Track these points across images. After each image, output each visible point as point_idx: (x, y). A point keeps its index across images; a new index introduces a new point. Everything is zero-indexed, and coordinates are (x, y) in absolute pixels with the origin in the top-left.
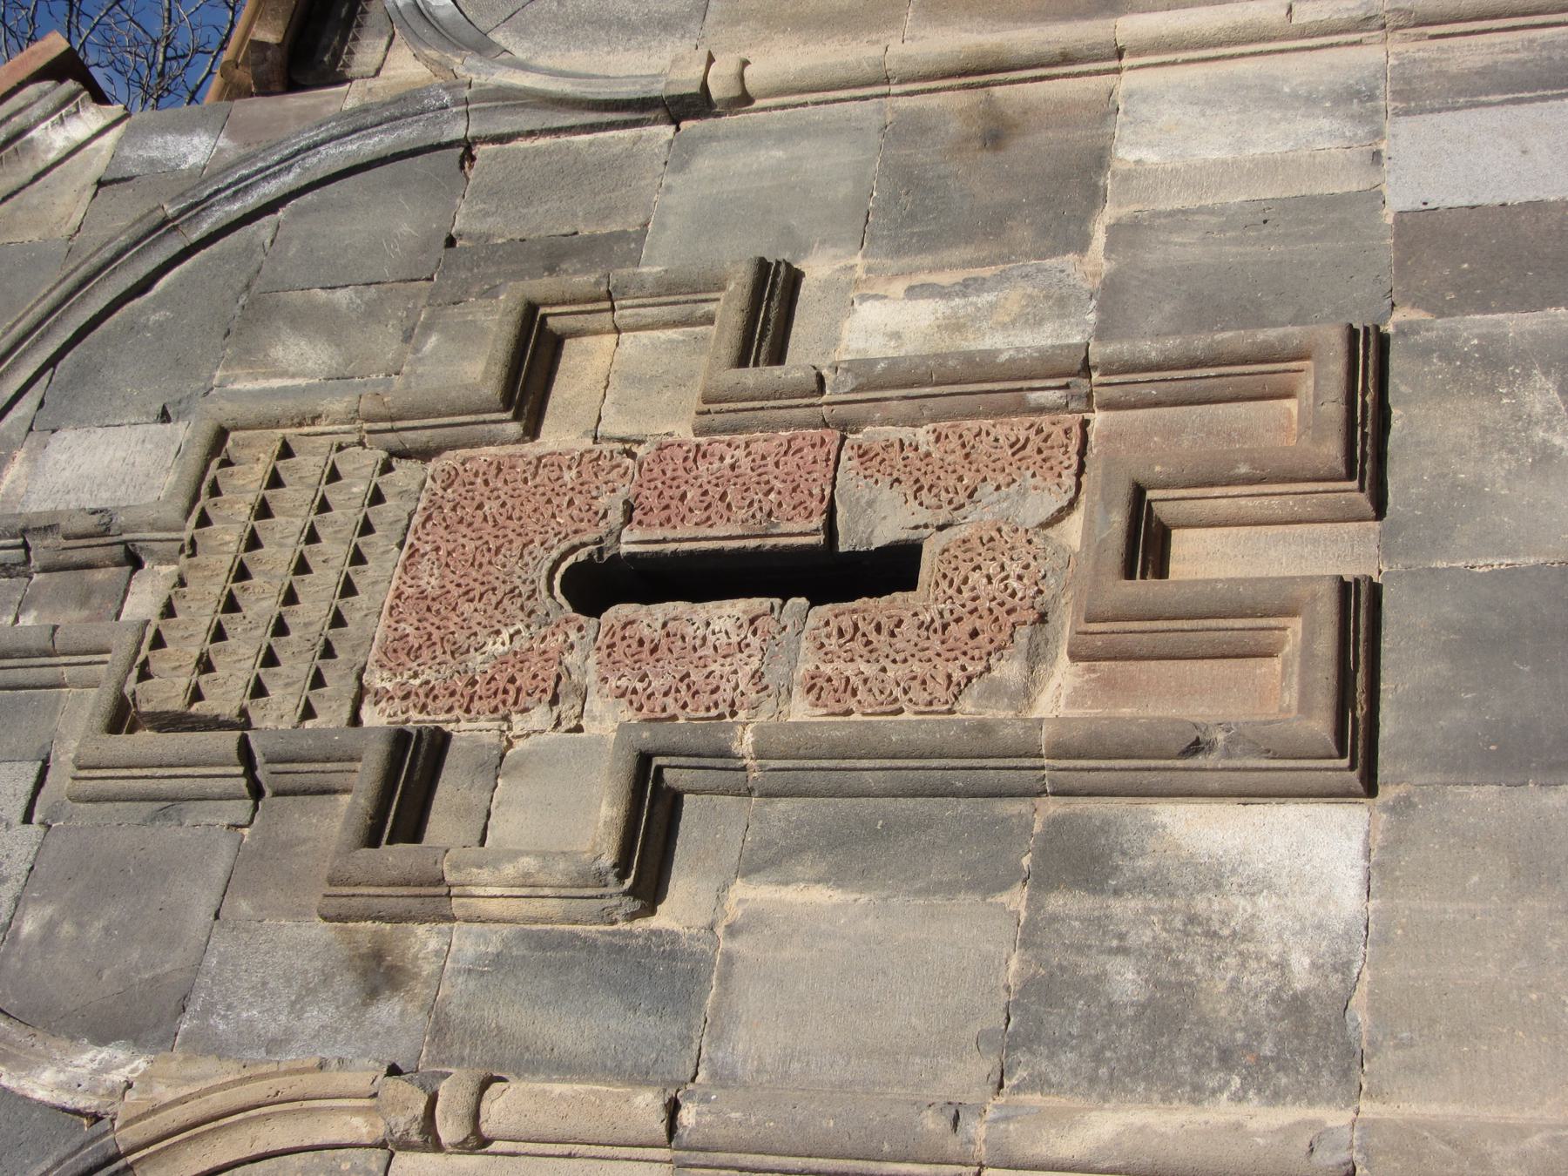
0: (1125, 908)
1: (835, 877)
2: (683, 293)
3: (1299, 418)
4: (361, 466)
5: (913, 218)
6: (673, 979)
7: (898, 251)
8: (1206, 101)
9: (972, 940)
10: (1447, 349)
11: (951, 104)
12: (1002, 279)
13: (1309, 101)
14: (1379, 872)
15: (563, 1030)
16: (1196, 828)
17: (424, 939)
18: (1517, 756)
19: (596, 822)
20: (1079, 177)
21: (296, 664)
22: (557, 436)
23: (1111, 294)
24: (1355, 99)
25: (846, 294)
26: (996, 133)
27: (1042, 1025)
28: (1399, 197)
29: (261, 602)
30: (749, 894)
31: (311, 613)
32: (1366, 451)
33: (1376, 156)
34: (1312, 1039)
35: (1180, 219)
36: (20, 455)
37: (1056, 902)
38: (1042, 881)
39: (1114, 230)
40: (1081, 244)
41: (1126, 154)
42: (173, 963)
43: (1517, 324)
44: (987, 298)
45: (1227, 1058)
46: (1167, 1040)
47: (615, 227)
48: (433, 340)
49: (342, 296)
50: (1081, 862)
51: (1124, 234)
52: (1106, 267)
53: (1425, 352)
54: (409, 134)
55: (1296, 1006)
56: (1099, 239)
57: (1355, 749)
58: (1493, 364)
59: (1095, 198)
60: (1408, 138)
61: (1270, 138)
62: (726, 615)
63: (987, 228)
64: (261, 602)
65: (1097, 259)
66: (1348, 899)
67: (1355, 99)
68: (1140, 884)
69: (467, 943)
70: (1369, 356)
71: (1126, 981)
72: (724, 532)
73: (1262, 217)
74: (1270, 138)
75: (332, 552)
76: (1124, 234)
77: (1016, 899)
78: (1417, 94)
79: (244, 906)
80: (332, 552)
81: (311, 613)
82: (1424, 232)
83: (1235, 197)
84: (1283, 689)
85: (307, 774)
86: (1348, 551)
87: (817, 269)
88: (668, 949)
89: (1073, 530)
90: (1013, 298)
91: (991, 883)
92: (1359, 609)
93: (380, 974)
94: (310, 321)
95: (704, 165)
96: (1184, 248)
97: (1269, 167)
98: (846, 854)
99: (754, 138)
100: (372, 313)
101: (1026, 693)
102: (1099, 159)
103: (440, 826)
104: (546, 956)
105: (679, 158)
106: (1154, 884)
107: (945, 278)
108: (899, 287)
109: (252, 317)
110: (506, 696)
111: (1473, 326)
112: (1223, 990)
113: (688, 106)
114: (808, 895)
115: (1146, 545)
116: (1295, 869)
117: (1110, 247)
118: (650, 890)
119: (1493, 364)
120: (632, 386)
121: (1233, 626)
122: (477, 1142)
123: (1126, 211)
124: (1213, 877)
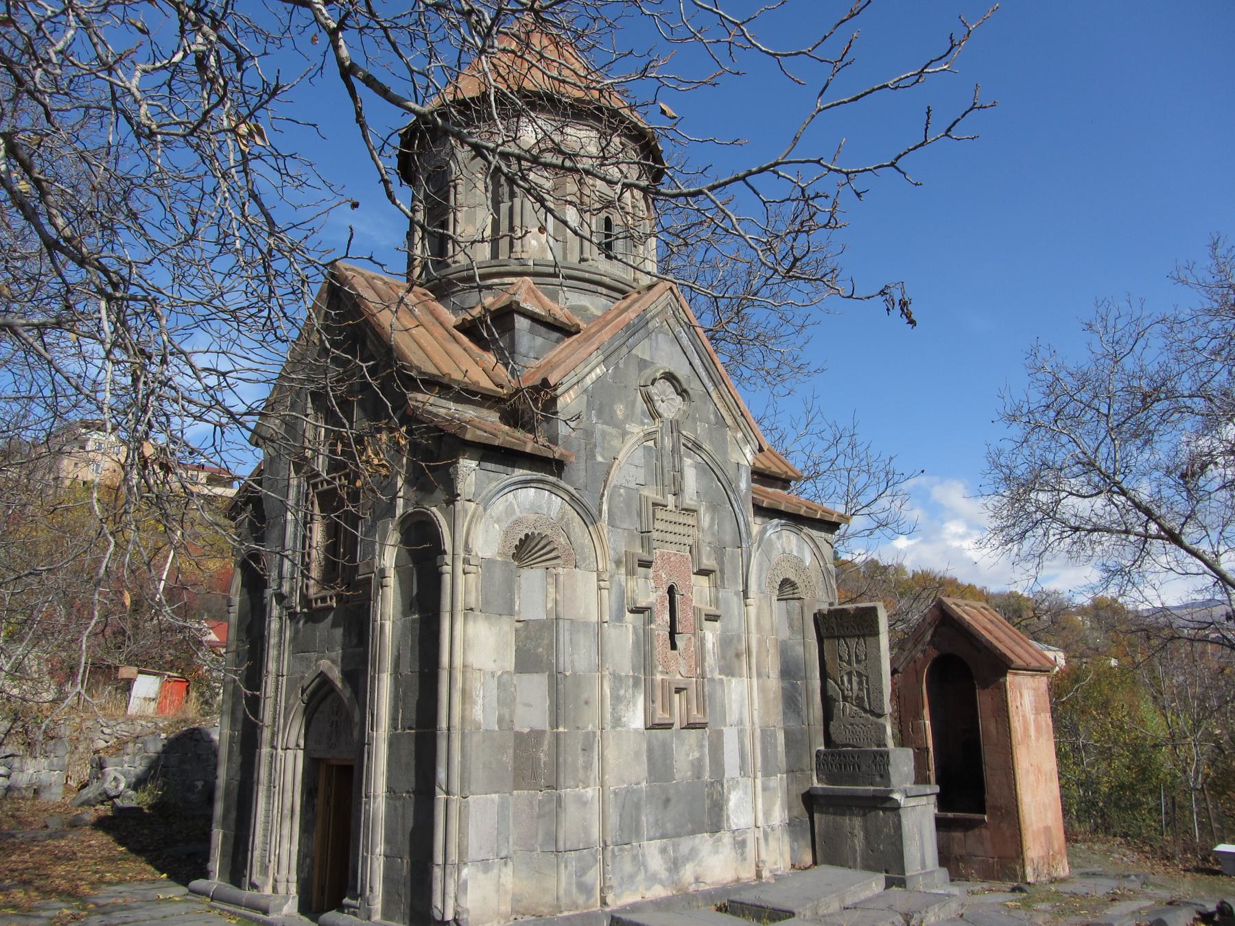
2: (716, 601)
4: (690, 541)
5: (726, 642)
6: (619, 617)
9: (626, 669)
11: (743, 646)
13: (741, 713)
14: (636, 730)
15: (613, 597)
17: (623, 570)
18: (650, 751)
19: (642, 603)
22: (693, 577)
23: (712, 680)
24: (741, 722)
25: (713, 630)
26: (738, 656)
27: (617, 679)
29: (671, 528)
30: (630, 627)
31: (669, 537)
32: (691, 726)
34: (617, 721)
38: (634, 677)
41: (734, 680)
42: (618, 522)
43: (706, 750)
51: (722, 680)
54: (744, 535)
57: (652, 726)
58: (701, 746)
59: (727, 675)
61: (735, 707)
62: (667, 617)
63: (723, 657)
64: (671, 528)
65: (717, 676)
66: (633, 726)
67: (741, 722)
69: (623, 578)
70: (702, 726)
71: (622, 692)
72: (679, 614)
73: (723, 706)
74: (735, 707)
75: (677, 539)
76: (722, 680)
77: (631, 673)
78: (741, 733)
80: (677, 539)
81: (669, 537)
82: (720, 734)
85: (646, 544)
86: (677, 726)
87: (717, 624)
88: (623, 615)
89: (679, 677)
91: (633, 670)
92: (668, 726)
93: (618, 563)
94: (712, 519)
95: (735, 599)
96: (719, 693)
97: (731, 707)
98: (636, 644)
99: (739, 609)
100: (713, 534)
102: (733, 676)
104: (622, 593)
105: (737, 594)
106: (634, 696)
109: (714, 508)
111: (706, 743)
112: (622, 707)
113: (746, 596)
115: (678, 691)
116: (636, 719)
118: (632, 611)
119: (701, 746)
120: (699, 591)
121: (668, 706)
122: (600, 588)
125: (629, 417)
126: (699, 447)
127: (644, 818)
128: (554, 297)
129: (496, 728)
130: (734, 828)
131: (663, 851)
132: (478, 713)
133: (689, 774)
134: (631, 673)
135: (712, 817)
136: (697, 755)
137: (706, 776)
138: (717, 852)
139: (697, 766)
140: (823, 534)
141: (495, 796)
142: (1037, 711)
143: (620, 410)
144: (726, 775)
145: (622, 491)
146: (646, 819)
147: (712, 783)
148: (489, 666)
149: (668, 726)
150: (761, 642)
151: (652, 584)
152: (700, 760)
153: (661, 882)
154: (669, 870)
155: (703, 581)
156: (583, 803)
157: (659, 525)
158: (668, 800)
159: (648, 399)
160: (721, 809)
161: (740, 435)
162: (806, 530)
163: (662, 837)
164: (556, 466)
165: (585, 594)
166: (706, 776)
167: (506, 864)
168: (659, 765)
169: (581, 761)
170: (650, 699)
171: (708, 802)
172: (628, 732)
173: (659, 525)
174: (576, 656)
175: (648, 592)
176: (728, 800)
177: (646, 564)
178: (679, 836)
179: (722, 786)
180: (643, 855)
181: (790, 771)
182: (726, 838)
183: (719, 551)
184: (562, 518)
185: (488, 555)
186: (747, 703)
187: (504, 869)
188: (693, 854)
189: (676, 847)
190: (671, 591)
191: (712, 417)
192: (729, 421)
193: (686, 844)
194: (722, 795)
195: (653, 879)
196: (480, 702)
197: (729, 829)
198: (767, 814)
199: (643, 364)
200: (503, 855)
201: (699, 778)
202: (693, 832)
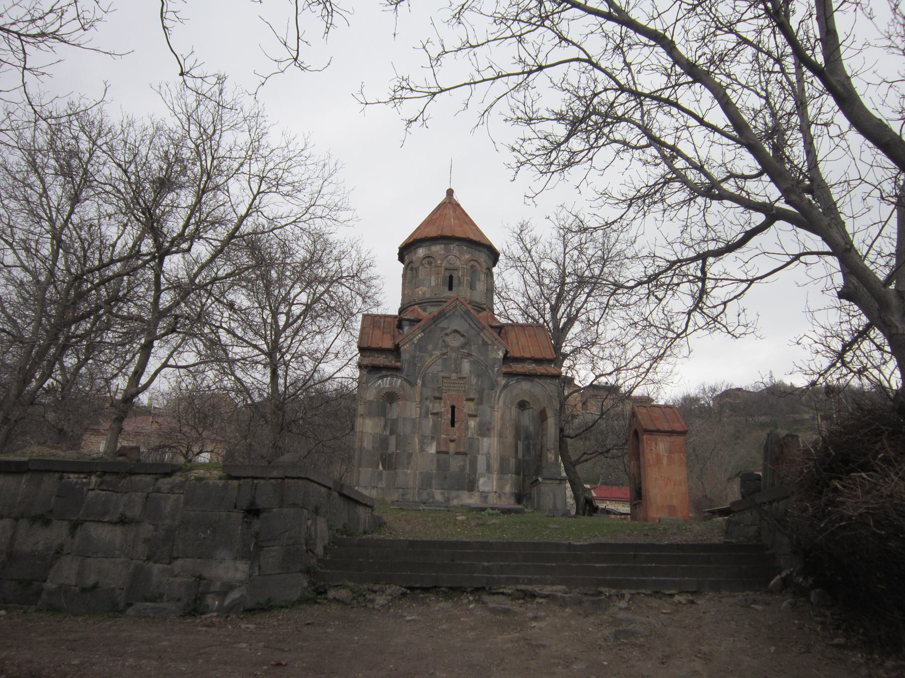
3: (462, 450)
6: (426, 416)
15: (423, 411)
16: (434, 444)
18: (438, 461)
19: (435, 411)
20: (484, 436)
22: (465, 402)
24: (488, 453)
32: (457, 453)
34: (422, 450)
50: (433, 438)
57: (438, 452)
62: (450, 416)
65: (476, 437)
67: (488, 453)
70: (465, 454)
82: (476, 458)
84: (443, 449)
87: (478, 419)
92: (447, 453)
94: (478, 381)
102: (485, 436)
109: (478, 376)
110: (445, 403)
114: (431, 423)
116: (432, 449)
119: (465, 461)
120: (469, 407)
125: (433, 350)
128: (425, 310)
131: (443, 494)
132: (365, 444)
135: (471, 486)
137: (467, 471)
139: (463, 468)
142: (670, 452)
143: (430, 347)
146: (434, 482)
148: (370, 431)
149: (447, 453)
150: (503, 426)
151: (443, 405)
155: (471, 404)
156: (406, 474)
158: (445, 478)
159: (444, 341)
163: (443, 489)
164: (397, 369)
165: (412, 410)
166: (467, 471)
168: (442, 466)
170: (438, 444)
171: (467, 481)
174: (405, 429)
175: (442, 408)
176: (478, 481)
177: (440, 398)
181: (518, 474)
182: (477, 494)
183: (481, 392)
186: (490, 446)
190: (453, 408)
191: (481, 343)
192: (490, 342)
193: (454, 493)
198: (501, 487)
199: (443, 329)
202: (459, 490)
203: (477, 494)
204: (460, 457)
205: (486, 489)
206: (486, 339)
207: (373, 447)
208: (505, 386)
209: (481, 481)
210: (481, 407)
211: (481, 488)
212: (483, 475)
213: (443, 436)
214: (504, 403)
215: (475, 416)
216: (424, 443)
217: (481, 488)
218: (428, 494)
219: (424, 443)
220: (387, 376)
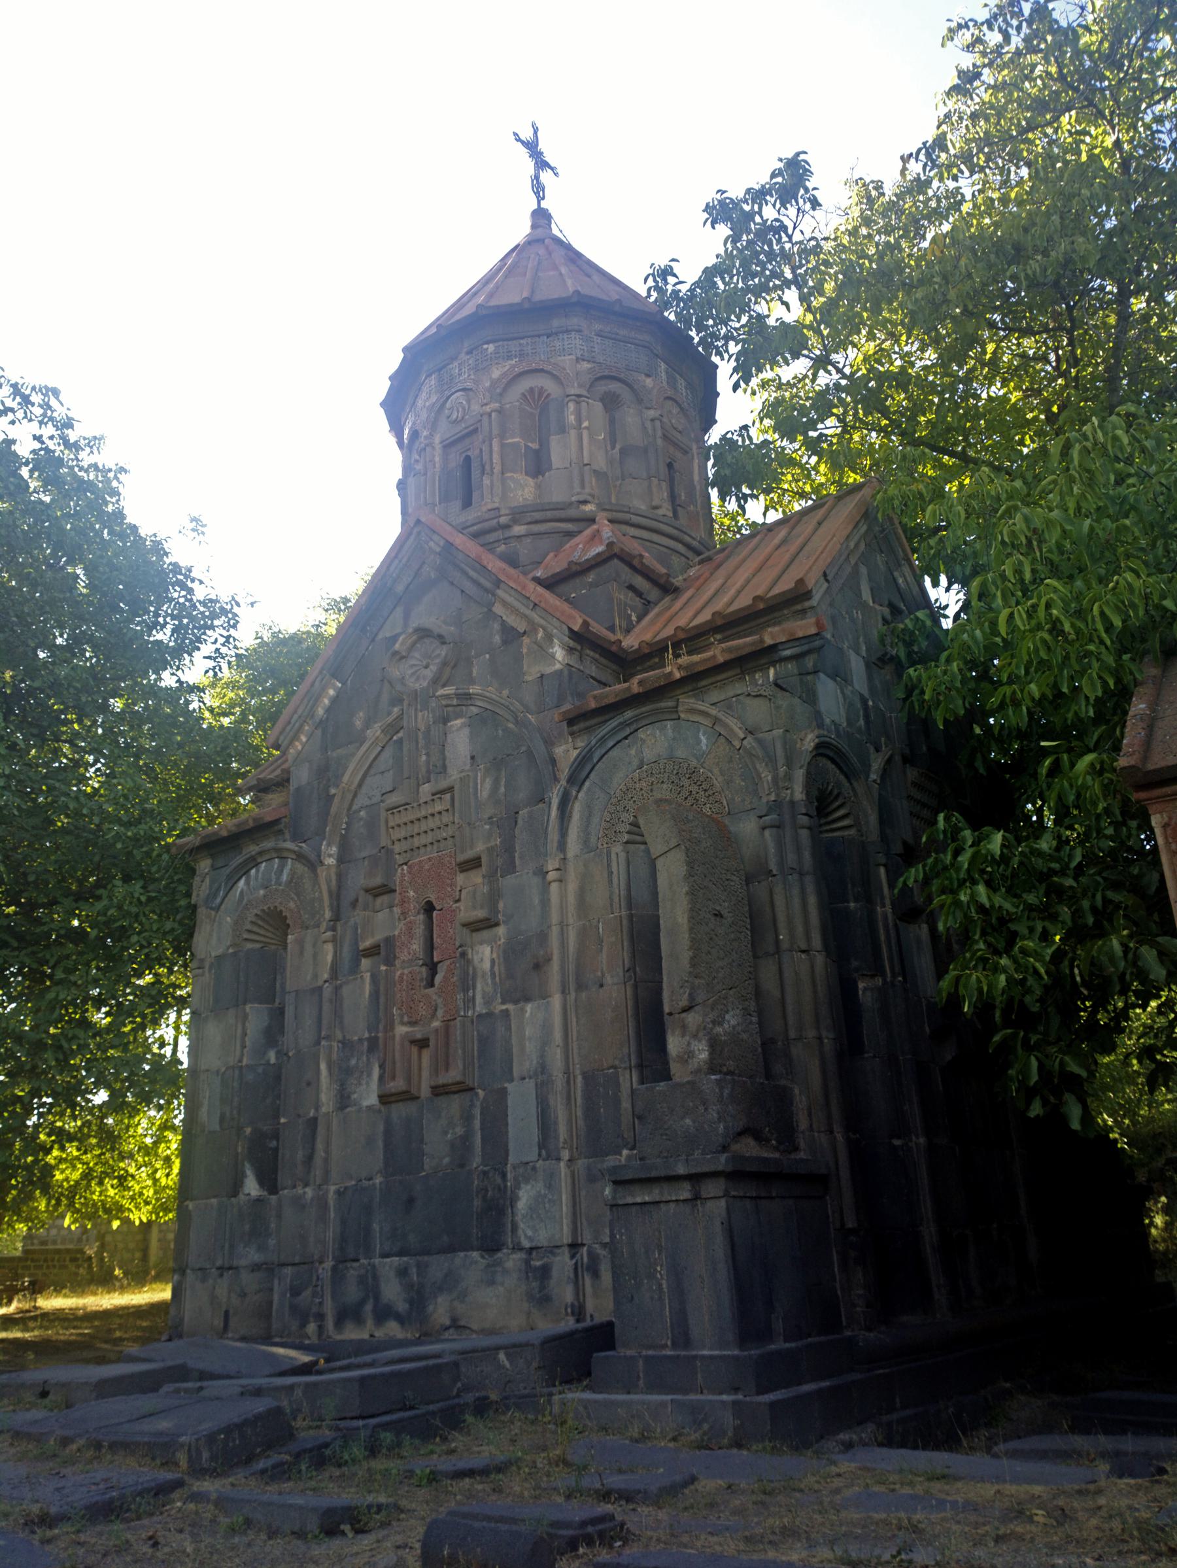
0: (365, 1058)
1: (371, 995)
5: (511, 953)
7: (505, 952)
8: (546, 1028)
10: (472, 1106)
12: (494, 983)
14: (369, 1108)
18: (388, 1133)
21: (405, 845)
22: (460, 879)
24: (543, 1068)
28: (510, 1087)
31: (417, 842)
33: (524, 1079)
34: (344, 1100)
35: (509, 1029)
36: (463, 720)
37: (366, 1043)
38: (369, 1039)
39: (507, 1010)
40: (503, 1003)
41: (529, 1008)
43: (477, 1123)
44: (489, 981)
45: (342, 1085)
46: (344, 1075)
47: (517, 862)
48: (487, 827)
49: (502, 789)
52: (497, 1011)
53: (471, 1101)
55: (349, 1097)
56: (504, 1007)
59: (516, 1002)
60: (530, 1084)
66: (365, 1103)
67: (543, 1068)
68: (368, 1060)
71: (353, 1062)
74: (531, 1047)
79: (366, 863)
83: (514, 1041)
86: (425, 1092)
87: (501, 931)
90: (489, 989)
101: (403, 1024)
102: (527, 999)
103: (379, 900)
107: (496, 969)
108: (495, 956)
111: (477, 1112)
117: (502, 1011)
118: (365, 956)
119: (467, 1118)
123: (512, 1013)
124: (369, 1075)
126: (468, 696)
127: (376, 1227)
129: (217, 1128)
130: (526, 1244)
131: (403, 1272)
133: (447, 1160)
134: (367, 1035)
136: (460, 1131)
137: (476, 1161)
138: (492, 1283)
140: (739, 688)
141: (214, 1201)
144: (512, 1159)
145: (362, 813)
147: (485, 1173)
149: (407, 1096)
152: (466, 1138)
153: (401, 1320)
154: (411, 1302)
156: (299, 1204)
157: (396, 834)
158: (411, 1201)
160: (501, 1212)
161: (540, 634)
162: (687, 701)
163: (400, 1254)
167: (221, 1275)
169: (300, 1155)
171: (477, 1203)
172: (360, 1110)
173: (396, 834)
176: (514, 1200)
178: (429, 1253)
179: (504, 1175)
180: (375, 1278)
182: (512, 1261)
184: (292, 879)
185: (219, 952)
186: (547, 1037)
187: (219, 1281)
188: (450, 1282)
189: (422, 1268)
193: (438, 1266)
194: (502, 1190)
195: (383, 1314)
196: (206, 1102)
197: (517, 1248)
200: (219, 1263)
201: (462, 1166)
202: (451, 1249)
203: (512, 1261)
204: (455, 1104)
205: (543, 1237)
206: (512, 620)
207: (222, 1119)
208: (576, 778)
209: (525, 1197)
210: (509, 882)
211: (527, 1233)
212: (528, 1171)
213: (401, 1030)
214: (586, 842)
215: (488, 924)
216: (348, 1071)
217: (527, 1233)
218: (362, 1280)
219: (348, 1071)
220: (253, 862)
